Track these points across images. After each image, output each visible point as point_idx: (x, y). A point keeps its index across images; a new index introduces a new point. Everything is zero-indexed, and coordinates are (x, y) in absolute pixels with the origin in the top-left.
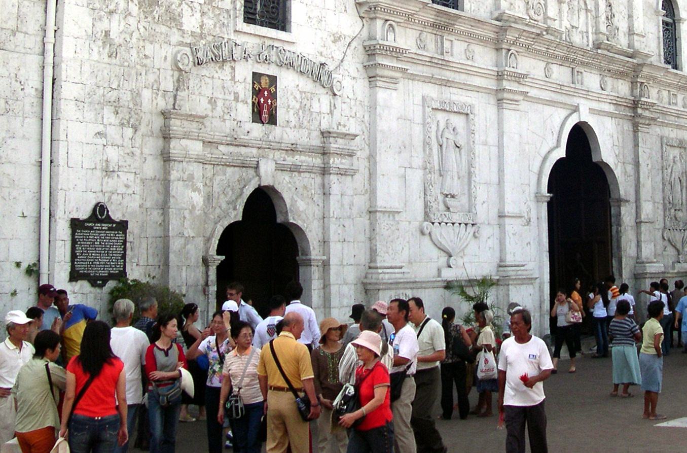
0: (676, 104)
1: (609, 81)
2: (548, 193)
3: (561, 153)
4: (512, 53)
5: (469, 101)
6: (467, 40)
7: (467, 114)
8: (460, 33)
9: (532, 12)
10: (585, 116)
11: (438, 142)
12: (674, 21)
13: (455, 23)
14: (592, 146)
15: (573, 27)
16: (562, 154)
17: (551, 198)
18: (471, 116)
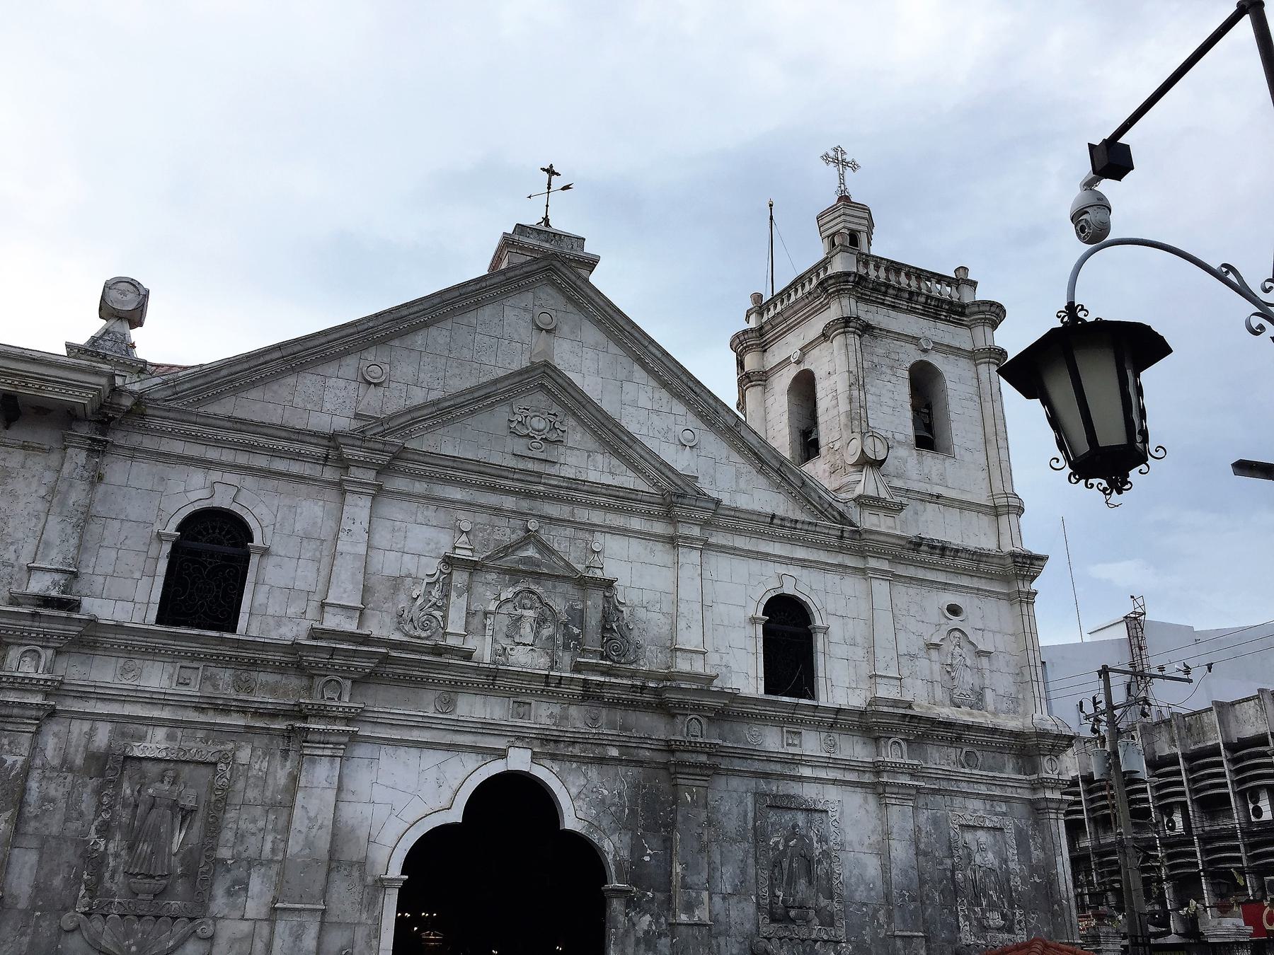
3: (456, 816)
10: (519, 760)
15: (518, 644)
16: (456, 816)
17: (405, 882)
18: (221, 766)
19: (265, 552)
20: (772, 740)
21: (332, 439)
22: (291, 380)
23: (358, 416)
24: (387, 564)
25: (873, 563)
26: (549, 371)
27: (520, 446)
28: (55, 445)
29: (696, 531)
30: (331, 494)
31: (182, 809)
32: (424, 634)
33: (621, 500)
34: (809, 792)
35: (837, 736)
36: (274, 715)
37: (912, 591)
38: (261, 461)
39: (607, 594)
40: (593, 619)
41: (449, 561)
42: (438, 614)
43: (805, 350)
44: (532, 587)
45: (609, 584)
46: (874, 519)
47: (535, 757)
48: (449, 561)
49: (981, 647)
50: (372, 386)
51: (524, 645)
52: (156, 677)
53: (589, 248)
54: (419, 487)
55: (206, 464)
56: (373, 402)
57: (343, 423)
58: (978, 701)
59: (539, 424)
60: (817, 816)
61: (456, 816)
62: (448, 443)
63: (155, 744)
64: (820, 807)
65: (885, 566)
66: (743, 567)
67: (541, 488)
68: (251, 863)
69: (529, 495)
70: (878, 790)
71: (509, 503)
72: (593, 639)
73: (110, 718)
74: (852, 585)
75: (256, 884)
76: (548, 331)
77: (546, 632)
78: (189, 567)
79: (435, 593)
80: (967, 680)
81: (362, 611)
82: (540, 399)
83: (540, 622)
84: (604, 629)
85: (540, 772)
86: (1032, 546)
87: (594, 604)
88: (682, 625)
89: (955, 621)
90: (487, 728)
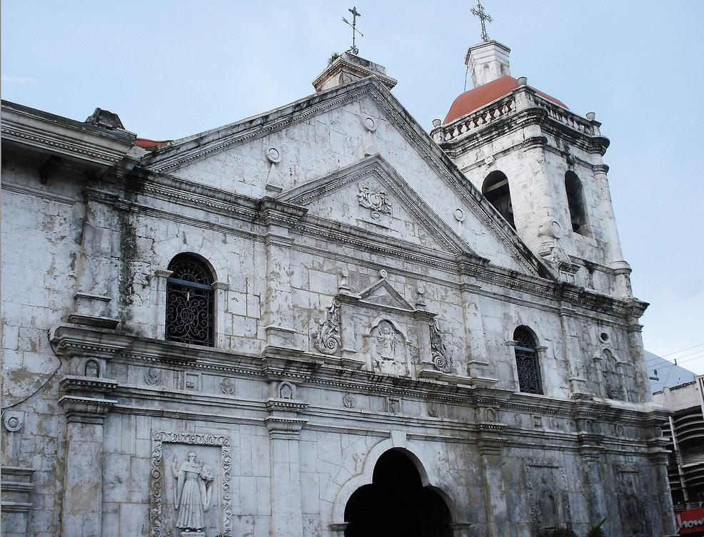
0: (541, 426)
1: (438, 407)
2: (345, 521)
3: (368, 479)
4: (285, 385)
5: (225, 433)
6: (222, 375)
7: (220, 446)
8: (205, 369)
9: (321, 347)
10: (399, 440)
11: (173, 475)
12: (536, 350)
13: (196, 358)
14: (420, 471)
15: (385, 359)
16: (370, 481)
17: (348, 525)
18: (223, 447)
21: (259, 205)
22: (222, 156)
23: (269, 188)
26: (379, 161)
27: (365, 215)
28: (77, 198)
30: (259, 246)
31: (205, 480)
32: (332, 351)
39: (430, 324)
41: (340, 298)
42: (337, 336)
43: (495, 156)
44: (388, 318)
45: (430, 317)
47: (409, 437)
48: (340, 298)
49: (619, 360)
50: (273, 165)
51: (389, 359)
53: (390, 74)
55: (177, 218)
56: (275, 176)
57: (258, 193)
59: (373, 200)
60: (554, 470)
61: (370, 481)
64: (555, 465)
67: (384, 246)
70: (579, 451)
74: (554, 318)
76: (372, 132)
78: (175, 298)
82: (372, 182)
85: (413, 447)
86: (639, 294)
88: (474, 345)
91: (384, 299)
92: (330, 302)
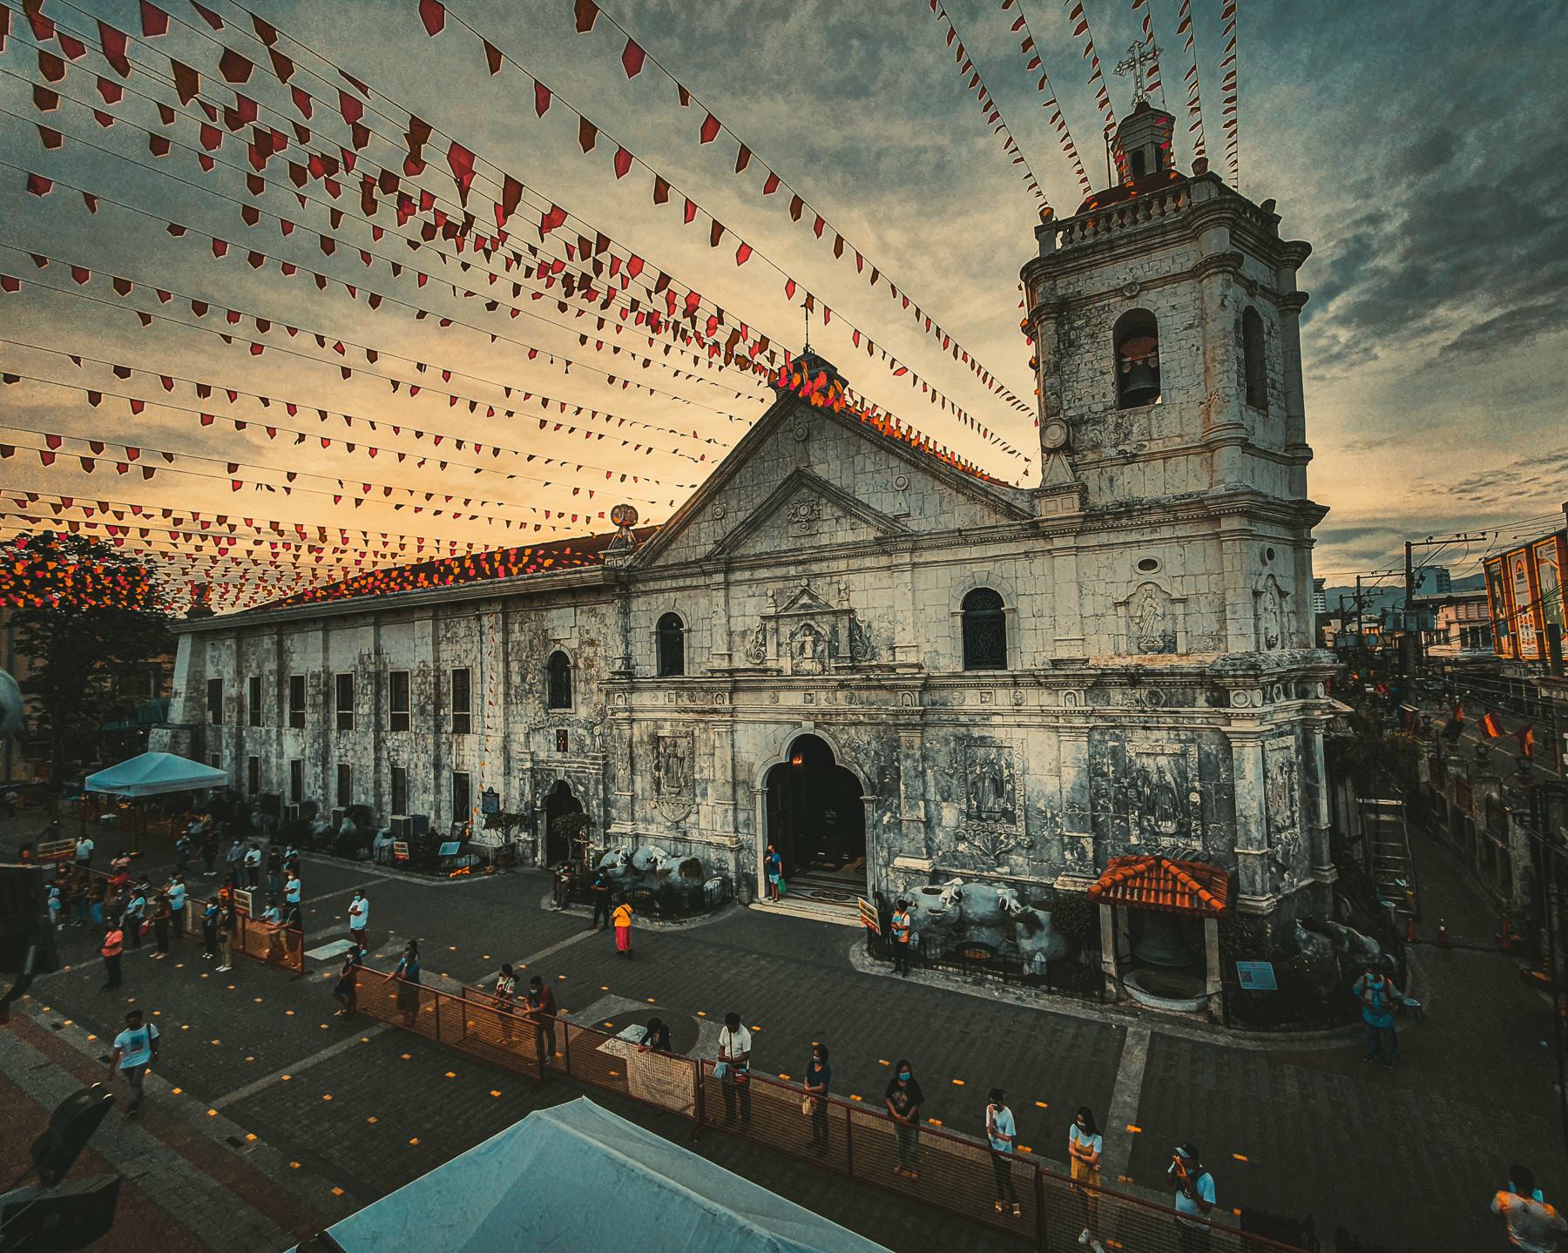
10: (808, 727)
19: (689, 631)
20: (971, 701)
24: (738, 625)
25: (1058, 542)
29: (906, 558)
33: (857, 550)
34: (998, 734)
35: (1023, 691)
36: (703, 712)
37: (1102, 558)
38: (681, 583)
40: (843, 634)
45: (851, 611)
46: (1052, 506)
47: (817, 725)
49: (1175, 595)
52: (661, 699)
54: (747, 575)
55: (661, 591)
58: (1170, 646)
59: (803, 511)
62: (761, 545)
63: (665, 732)
65: (1070, 541)
66: (944, 574)
68: (707, 781)
69: (801, 563)
71: (792, 571)
72: (844, 650)
73: (651, 720)
75: (710, 791)
77: (819, 649)
79: (760, 636)
80: (1157, 628)
81: (730, 656)
83: (815, 644)
84: (851, 641)
85: (820, 733)
87: (843, 625)
89: (1148, 575)
90: (791, 710)
91: (803, 606)
92: (756, 623)
